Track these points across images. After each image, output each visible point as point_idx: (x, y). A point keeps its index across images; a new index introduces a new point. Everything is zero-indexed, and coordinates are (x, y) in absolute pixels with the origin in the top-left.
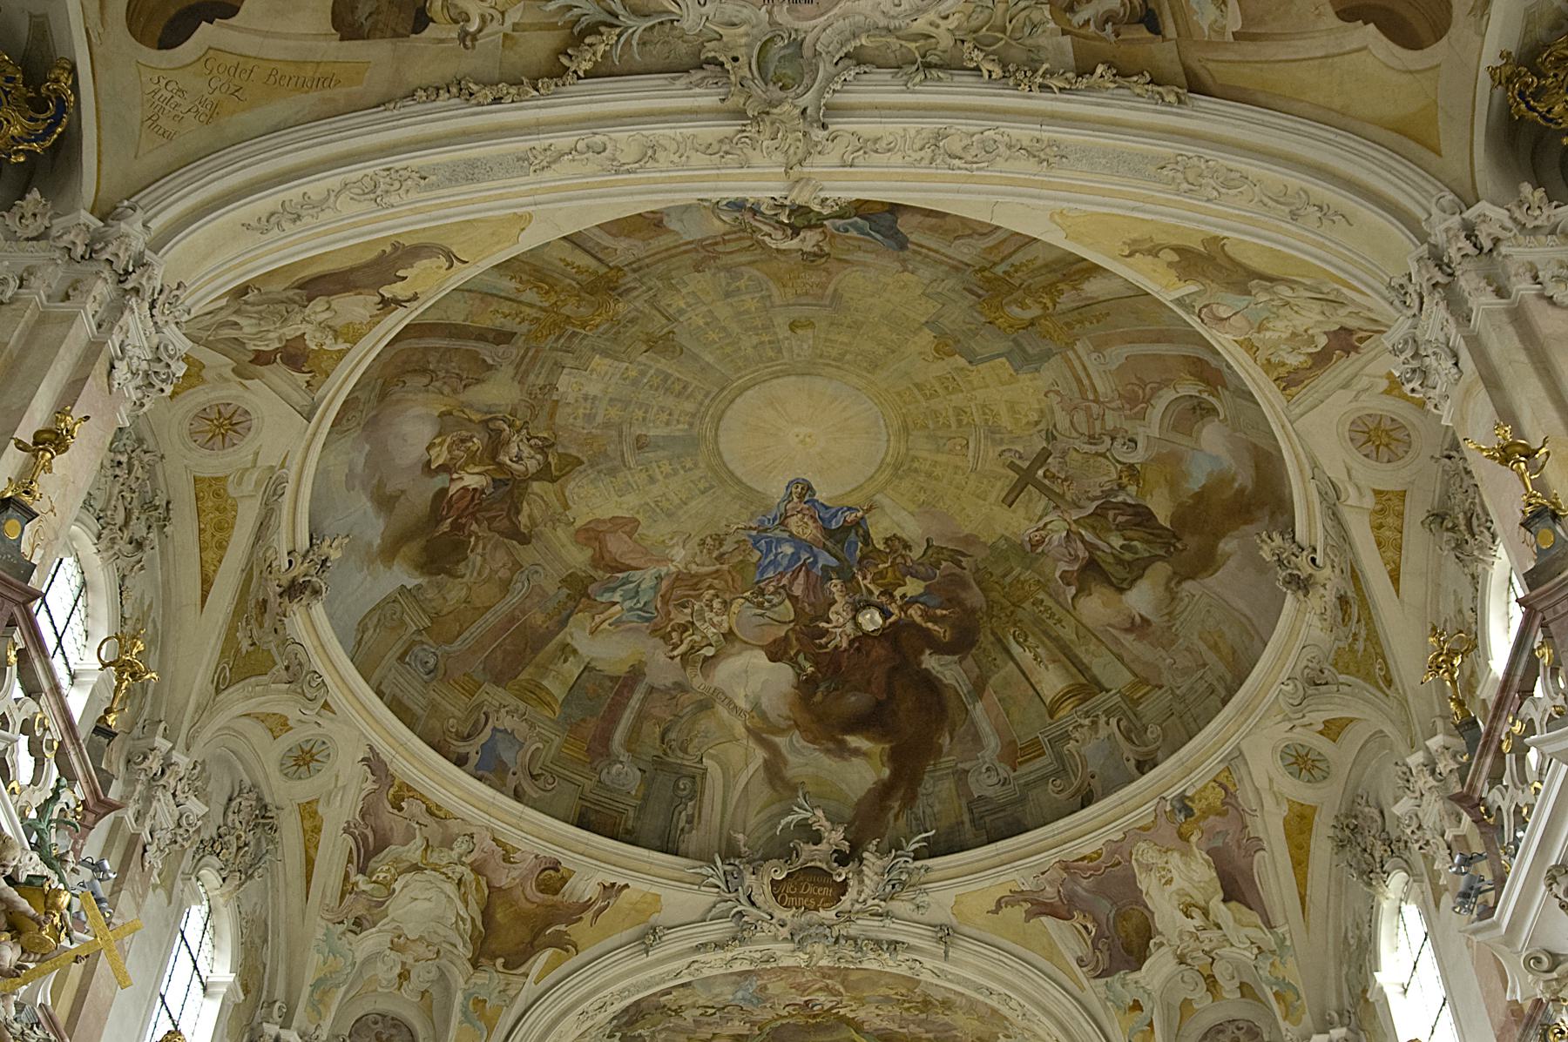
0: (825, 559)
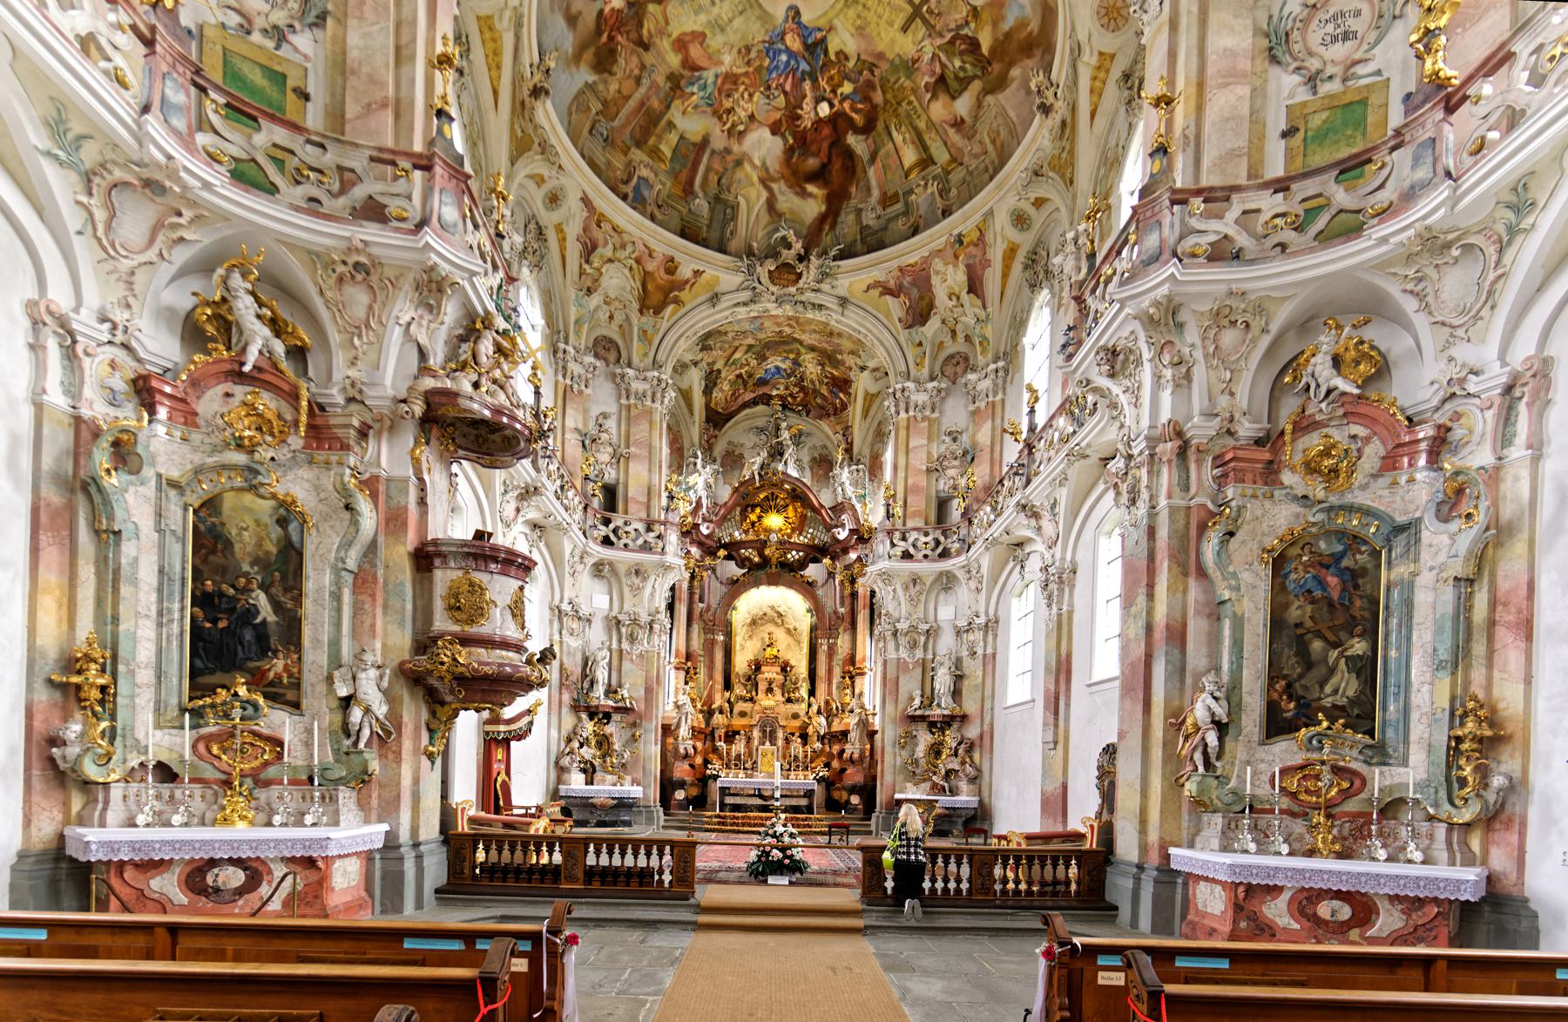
0: (804, 66)
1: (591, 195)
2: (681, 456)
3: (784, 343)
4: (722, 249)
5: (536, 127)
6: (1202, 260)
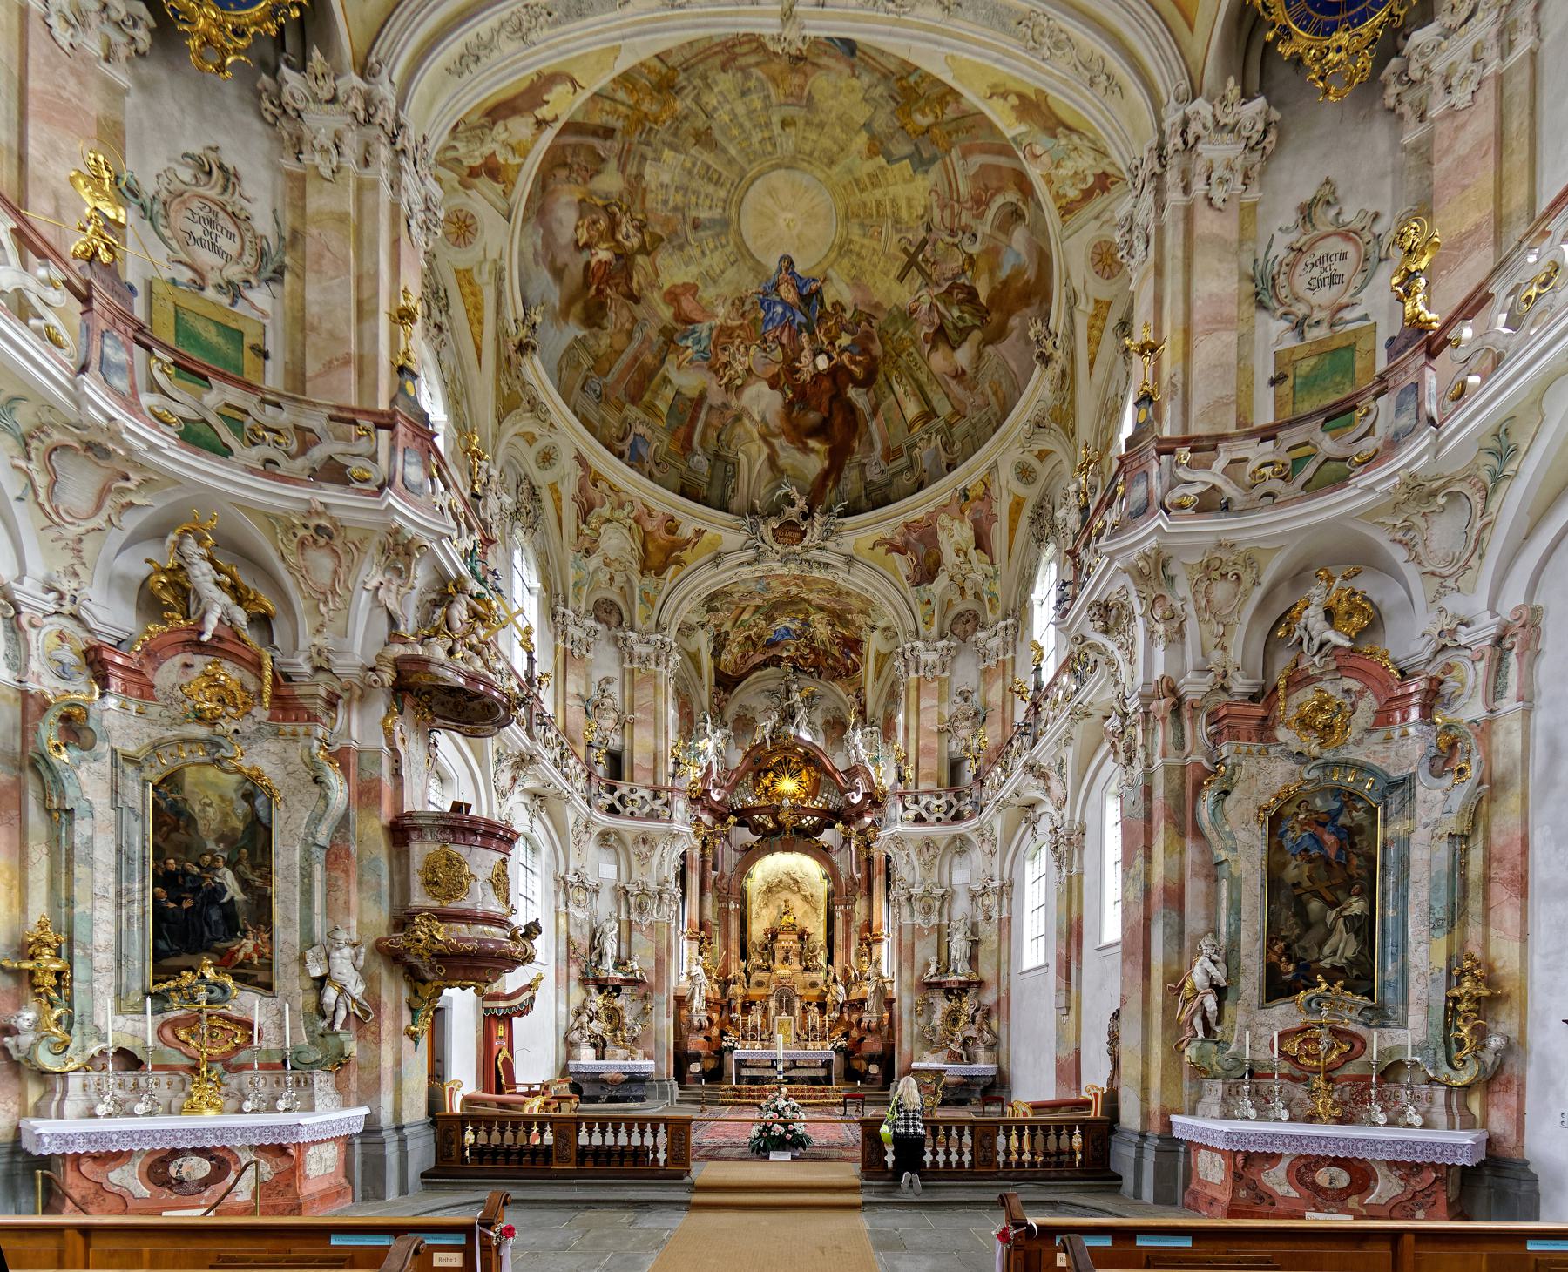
0: (800, 318)
1: (585, 453)
2: (691, 721)
3: (792, 603)
4: (726, 510)
5: (524, 384)
6: (1189, 511)
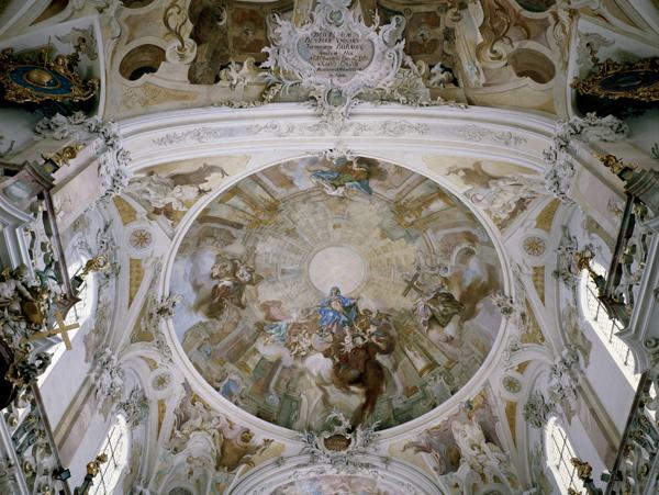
0: (343, 318)
1: (191, 381)
